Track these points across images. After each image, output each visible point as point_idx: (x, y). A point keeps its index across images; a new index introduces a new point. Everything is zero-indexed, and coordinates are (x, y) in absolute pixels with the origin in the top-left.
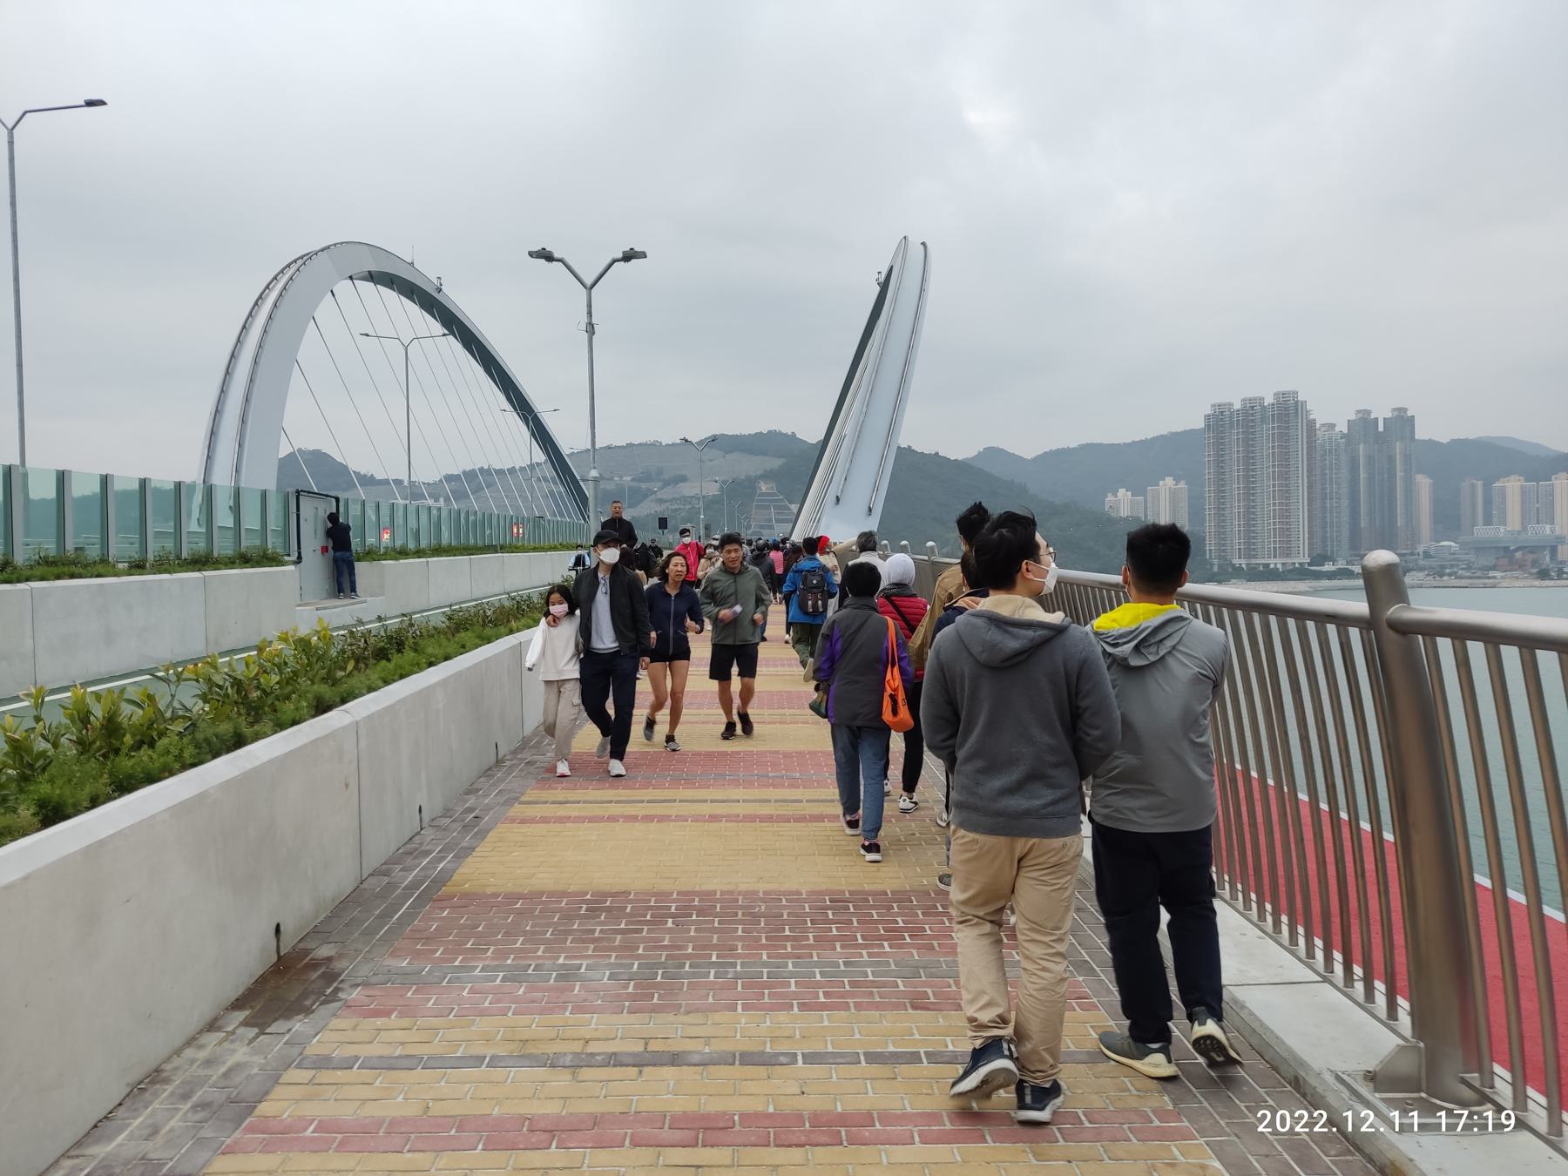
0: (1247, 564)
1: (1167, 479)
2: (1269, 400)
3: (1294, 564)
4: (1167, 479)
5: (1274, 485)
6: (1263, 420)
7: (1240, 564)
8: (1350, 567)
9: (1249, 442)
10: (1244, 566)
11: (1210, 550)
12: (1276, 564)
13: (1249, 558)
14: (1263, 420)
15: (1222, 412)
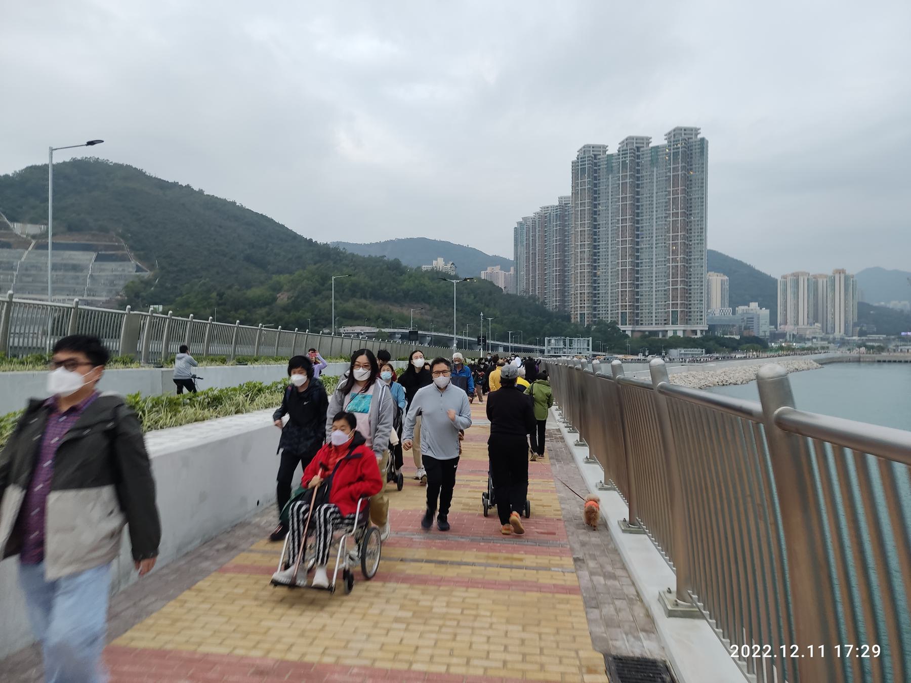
0: (633, 331)
1: (439, 259)
2: (658, 140)
3: (695, 332)
4: (439, 259)
5: (675, 238)
6: (654, 162)
7: (625, 331)
8: (734, 336)
9: (637, 187)
10: (629, 333)
11: (582, 315)
12: (675, 332)
13: (633, 324)
14: (654, 162)
15: (595, 155)
